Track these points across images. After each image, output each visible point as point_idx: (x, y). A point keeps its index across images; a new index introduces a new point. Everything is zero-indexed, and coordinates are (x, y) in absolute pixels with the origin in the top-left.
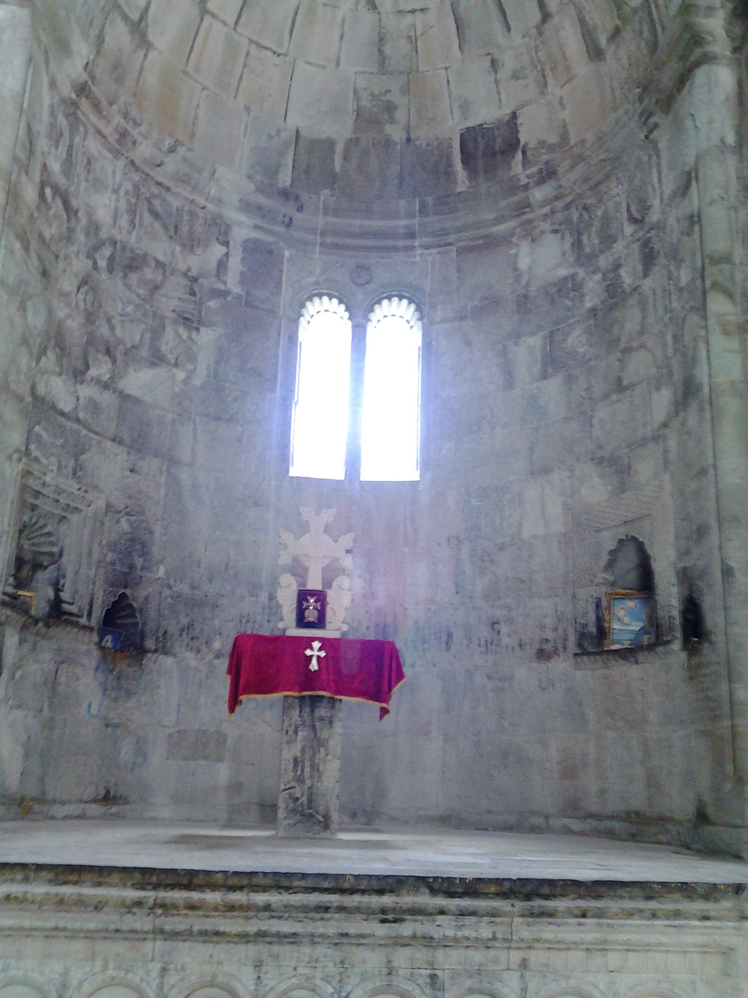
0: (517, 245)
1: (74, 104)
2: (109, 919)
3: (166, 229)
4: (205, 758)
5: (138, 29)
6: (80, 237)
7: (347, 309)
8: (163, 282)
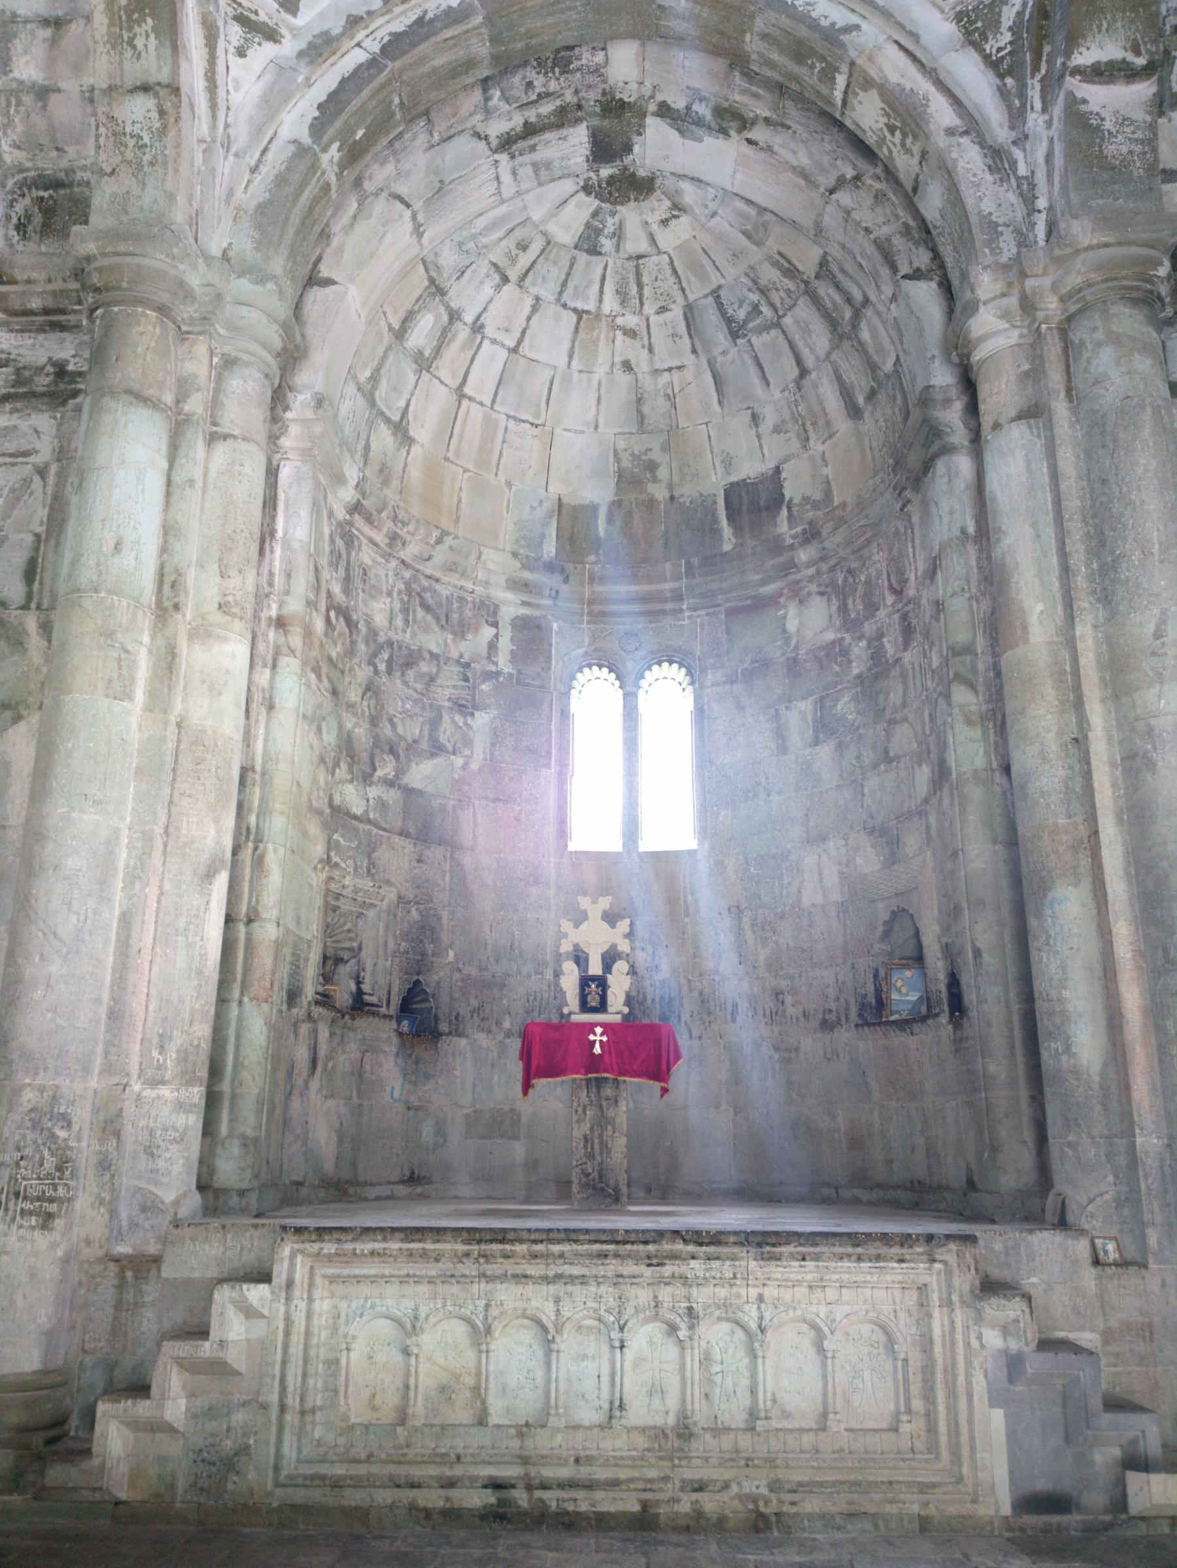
0: (785, 607)
1: (350, 523)
2: (446, 1266)
3: (438, 620)
4: (502, 1136)
5: (401, 430)
6: (362, 646)
7: (618, 678)
8: (437, 673)
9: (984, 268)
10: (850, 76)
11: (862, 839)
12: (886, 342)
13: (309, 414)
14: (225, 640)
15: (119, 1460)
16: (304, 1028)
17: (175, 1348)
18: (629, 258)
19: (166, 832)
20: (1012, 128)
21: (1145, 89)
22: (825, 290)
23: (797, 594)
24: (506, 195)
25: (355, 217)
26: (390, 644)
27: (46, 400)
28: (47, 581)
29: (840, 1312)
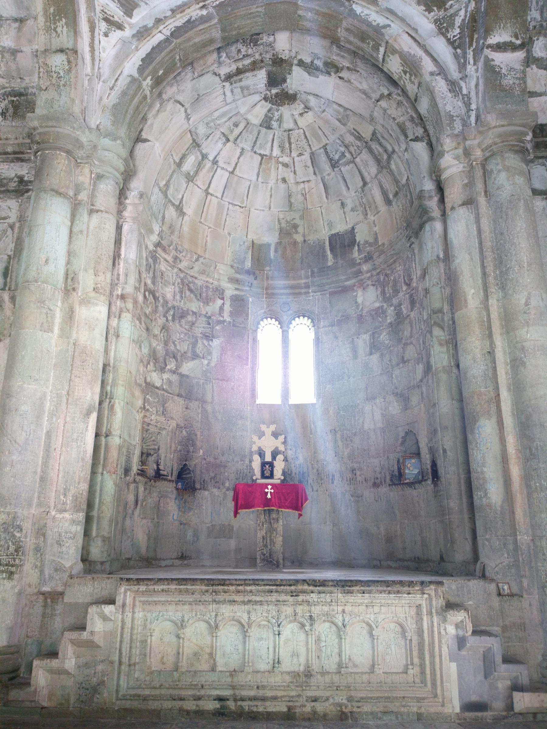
0: (357, 291)
1: (155, 252)
2: (197, 596)
3: (196, 296)
4: (225, 537)
5: (179, 209)
6: (160, 308)
7: (279, 324)
9: (447, 136)
10: (386, 48)
11: (392, 398)
12: (403, 169)
13: (137, 201)
14: (97, 305)
15: (43, 688)
16: (132, 486)
17: (69, 635)
18: (285, 131)
19: (68, 394)
20: (460, 72)
21: (520, 55)
22: (375, 146)
23: (362, 285)
24: (228, 102)
25: (158, 111)
26: (174, 307)
27: (14, 193)
28: (14, 277)
29: (380, 618)
